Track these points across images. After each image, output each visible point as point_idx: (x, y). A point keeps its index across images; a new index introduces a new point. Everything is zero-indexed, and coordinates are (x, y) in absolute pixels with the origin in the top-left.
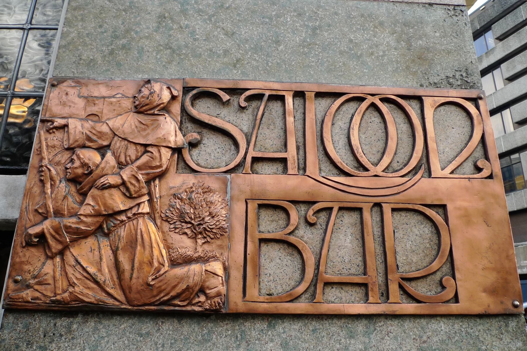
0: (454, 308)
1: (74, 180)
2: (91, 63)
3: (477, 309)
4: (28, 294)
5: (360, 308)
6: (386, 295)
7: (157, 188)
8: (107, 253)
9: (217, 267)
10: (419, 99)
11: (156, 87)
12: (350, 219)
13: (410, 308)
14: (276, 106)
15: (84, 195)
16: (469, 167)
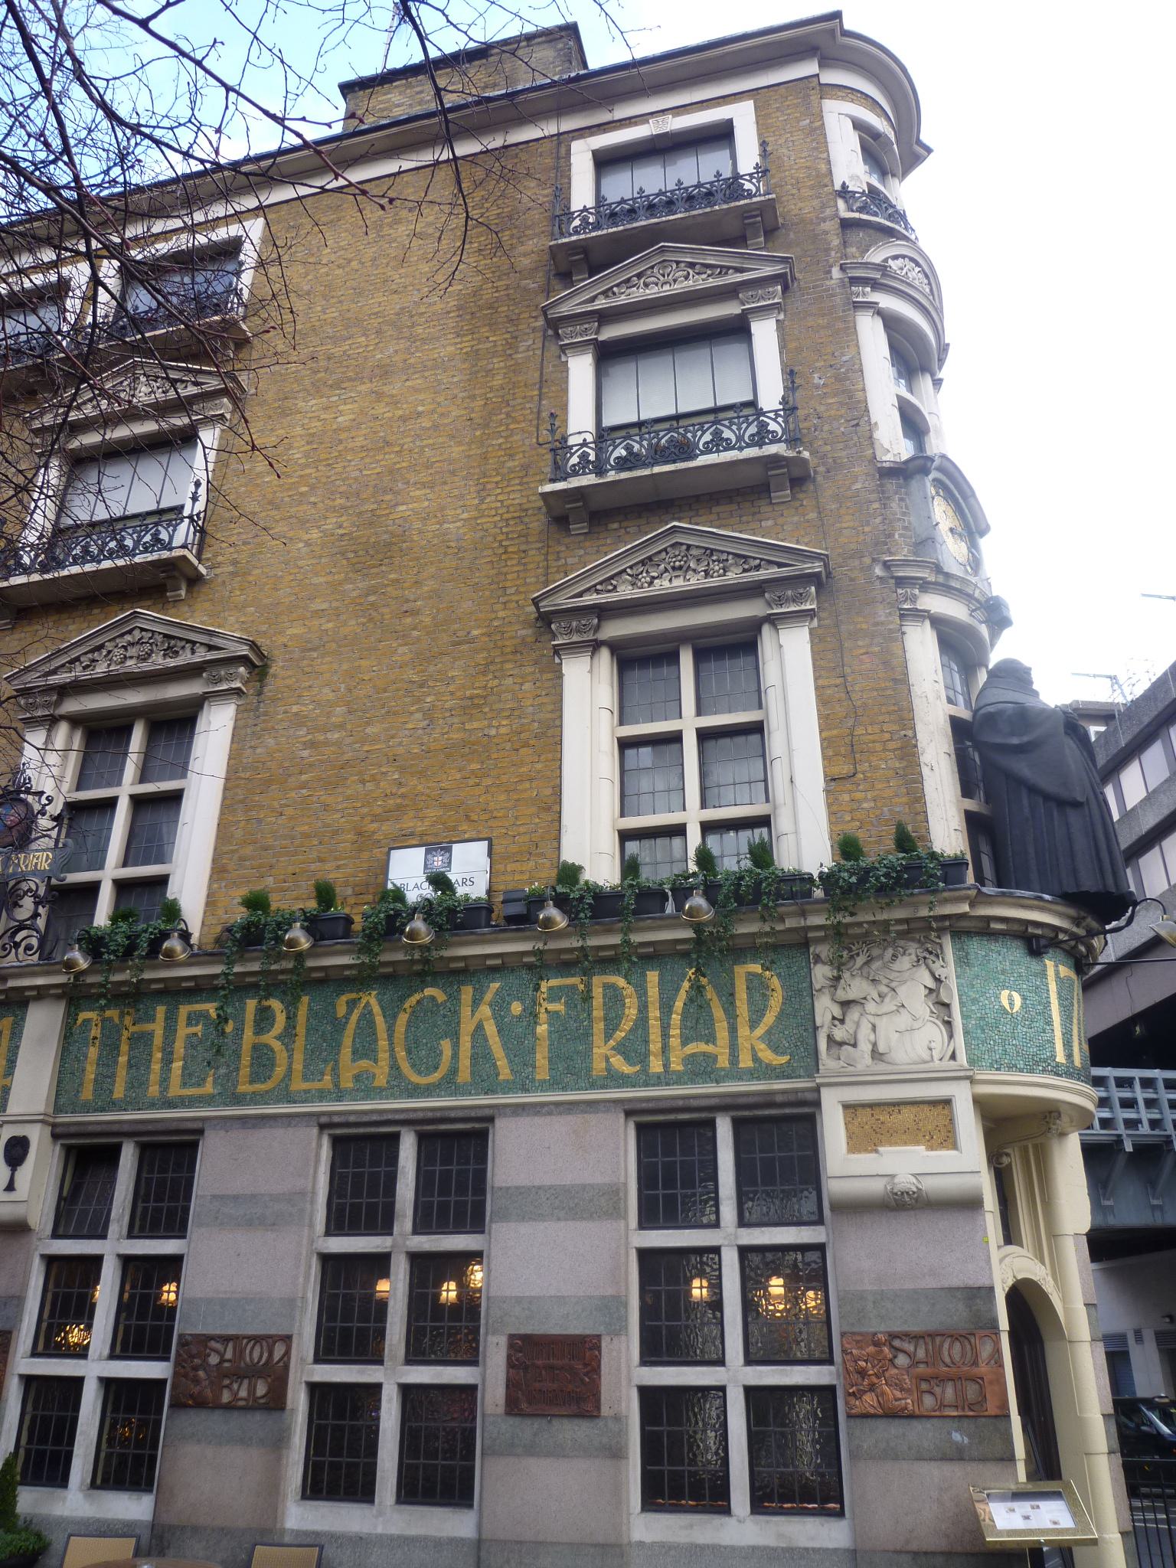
0: (986, 1413)
1: (859, 1373)
2: (853, 1324)
3: (993, 1413)
4: (853, 1411)
5: (955, 1414)
6: (963, 1409)
7: (887, 1374)
8: (875, 1398)
9: (909, 1401)
10: (974, 1335)
11: (880, 1336)
12: (950, 1383)
13: (971, 1413)
14: (921, 1342)
15: (863, 1379)
16: (993, 1362)
